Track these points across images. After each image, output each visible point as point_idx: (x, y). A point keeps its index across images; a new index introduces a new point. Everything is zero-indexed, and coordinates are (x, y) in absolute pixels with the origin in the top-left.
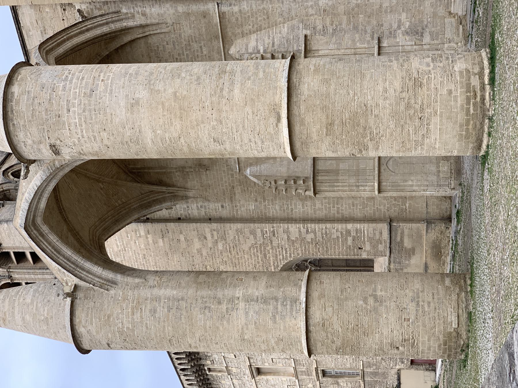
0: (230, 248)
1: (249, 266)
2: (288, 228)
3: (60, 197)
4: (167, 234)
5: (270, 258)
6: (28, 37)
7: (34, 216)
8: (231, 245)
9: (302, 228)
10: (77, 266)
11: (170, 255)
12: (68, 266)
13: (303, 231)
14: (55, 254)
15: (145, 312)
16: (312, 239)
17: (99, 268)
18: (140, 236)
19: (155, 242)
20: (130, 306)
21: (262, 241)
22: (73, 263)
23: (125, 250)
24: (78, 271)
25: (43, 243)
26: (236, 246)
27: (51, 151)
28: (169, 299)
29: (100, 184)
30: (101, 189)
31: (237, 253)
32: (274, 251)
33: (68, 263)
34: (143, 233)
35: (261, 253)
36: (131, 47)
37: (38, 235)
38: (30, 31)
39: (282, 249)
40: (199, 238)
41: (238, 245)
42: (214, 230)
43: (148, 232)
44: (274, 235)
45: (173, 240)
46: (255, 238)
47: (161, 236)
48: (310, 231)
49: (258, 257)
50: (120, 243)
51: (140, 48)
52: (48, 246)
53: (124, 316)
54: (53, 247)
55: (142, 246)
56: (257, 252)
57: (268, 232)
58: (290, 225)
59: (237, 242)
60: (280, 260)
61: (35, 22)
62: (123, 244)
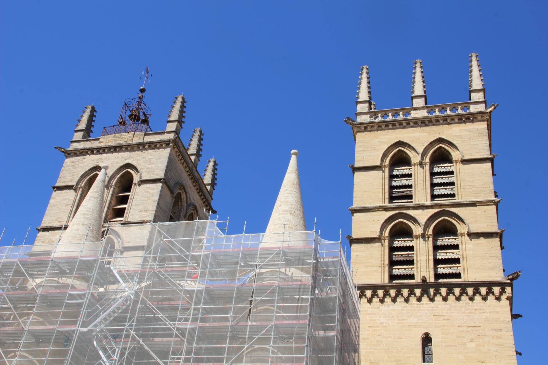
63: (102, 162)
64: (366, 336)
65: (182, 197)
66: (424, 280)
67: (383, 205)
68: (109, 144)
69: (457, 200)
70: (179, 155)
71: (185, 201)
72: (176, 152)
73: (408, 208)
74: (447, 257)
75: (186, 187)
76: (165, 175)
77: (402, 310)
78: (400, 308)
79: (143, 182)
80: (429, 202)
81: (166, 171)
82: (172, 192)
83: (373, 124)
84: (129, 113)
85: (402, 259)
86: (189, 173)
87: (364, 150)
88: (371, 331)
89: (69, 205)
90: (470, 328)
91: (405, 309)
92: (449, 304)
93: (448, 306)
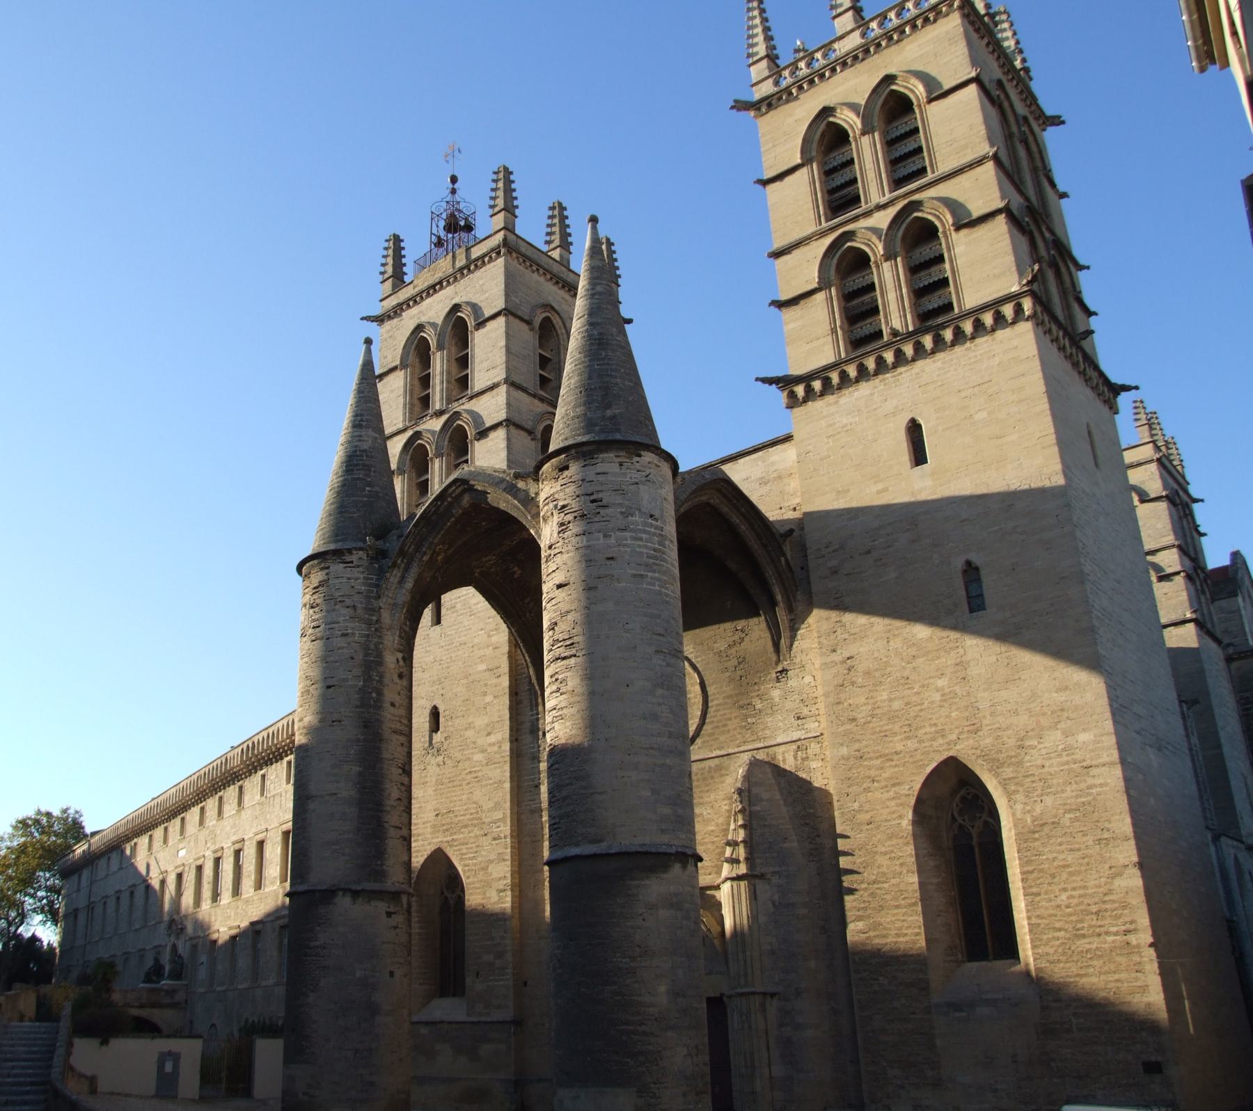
0: (475, 772)
1: (451, 802)
2: (504, 860)
4: (493, 676)
5: (463, 833)
6: (755, 459)
8: (480, 774)
9: (505, 882)
11: (464, 681)
13: (501, 885)
16: (489, 898)
18: (489, 636)
19: (482, 659)
21: (486, 820)
23: (471, 615)
26: (478, 781)
31: (469, 783)
32: (472, 840)
34: (494, 639)
35: (470, 820)
38: (763, 462)
39: (476, 852)
40: (487, 725)
41: (480, 783)
42: (500, 747)
43: (496, 648)
44: (495, 839)
45: (486, 685)
46: (489, 810)
47: (490, 667)
48: (501, 894)
49: (464, 815)
50: (481, 607)
55: (476, 640)
56: (471, 814)
57: (499, 829)
58: (509, 863)
59: (484, 783)
60: (459, 850)
61: (776, 468)
62: (479, 612)
63: (424, 315)
64: (825, 453)
65: (555, 322)
66: (895, 333)
67: (819, 228)
68: (426, 284)
69: (930, 176)
70: (524, 261)
71: (562, 326)
72: (518, 258)
73: (855, 219)
74: (931, 281)
75: (554, 305)
76: (506, 302)
77: (872, 394)
78: (868, 392)
79: (480, 324)
80: (888, 196)
81: (507, 295)
82: (528, 323)
83: (779, 95)
84: (442, 224)
85: (864, 309)
86: (554, 281)
87: (774, 146)
88: (831, 443)
89: (399, 396)
90: (976, 389)
91: (876, 390)
92: (939, 360)
93: (939, 364)
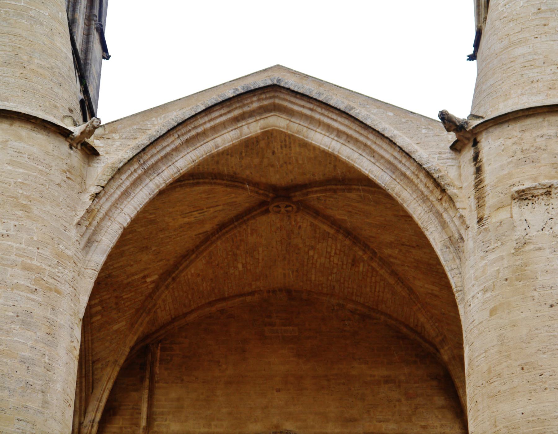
3: (219, 184)
7: (290, 113)
10: (146, 172)
12: (154, 151)
14: (190, 131)
15: (29, 299)
17: (129, 220)
20: (44, 266)
22: (156, 163)
24: (135, 171)
25: (225, 114)
27: (528, 184)
28: (48, 368)
29: (155, 277)
30: (145, 277)
33: (163, 154)
36: (443, 407)
37: (246, 109)
51: (442, 426)
52: (212, 124)
53: (23, 246)
54: (204, 133)
